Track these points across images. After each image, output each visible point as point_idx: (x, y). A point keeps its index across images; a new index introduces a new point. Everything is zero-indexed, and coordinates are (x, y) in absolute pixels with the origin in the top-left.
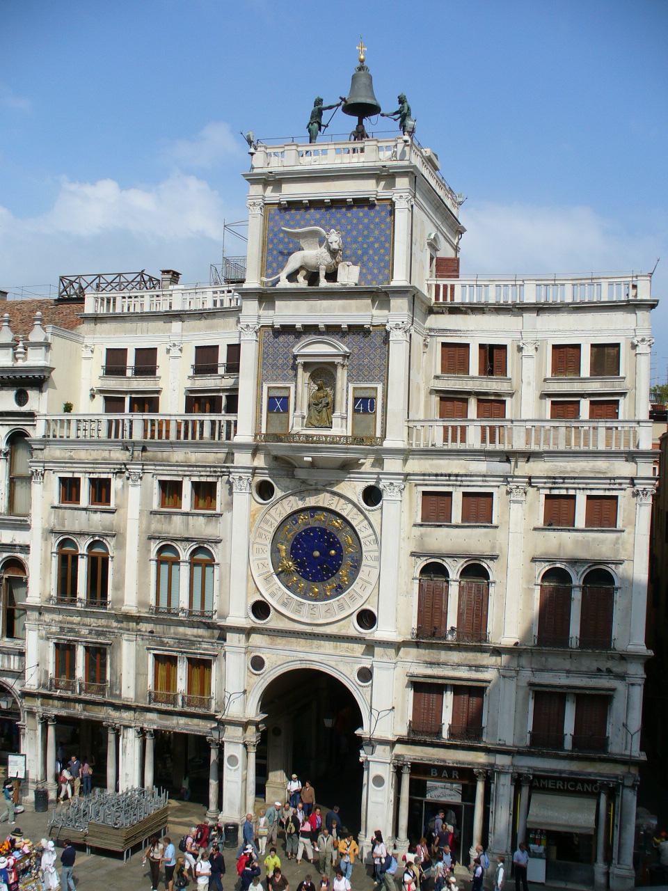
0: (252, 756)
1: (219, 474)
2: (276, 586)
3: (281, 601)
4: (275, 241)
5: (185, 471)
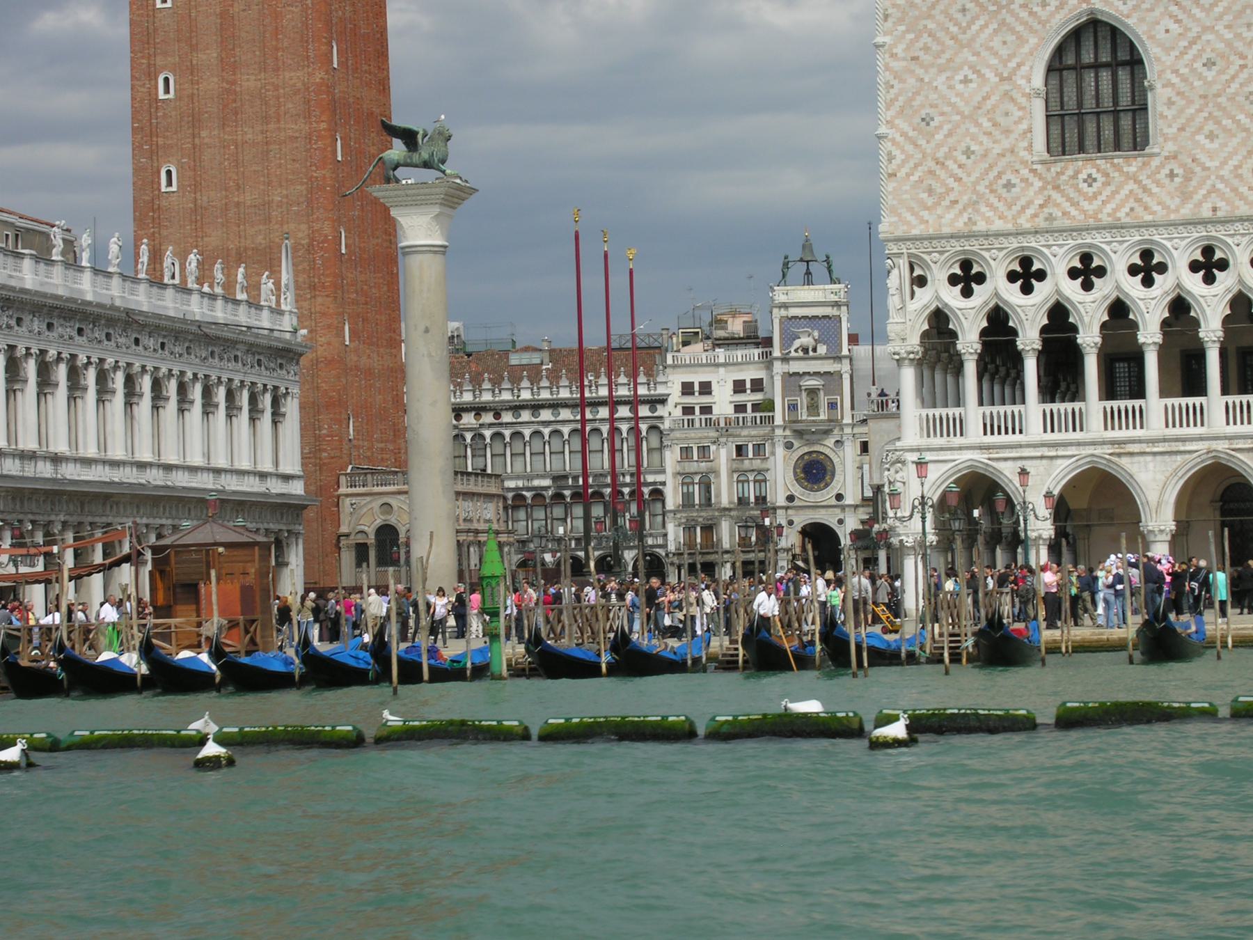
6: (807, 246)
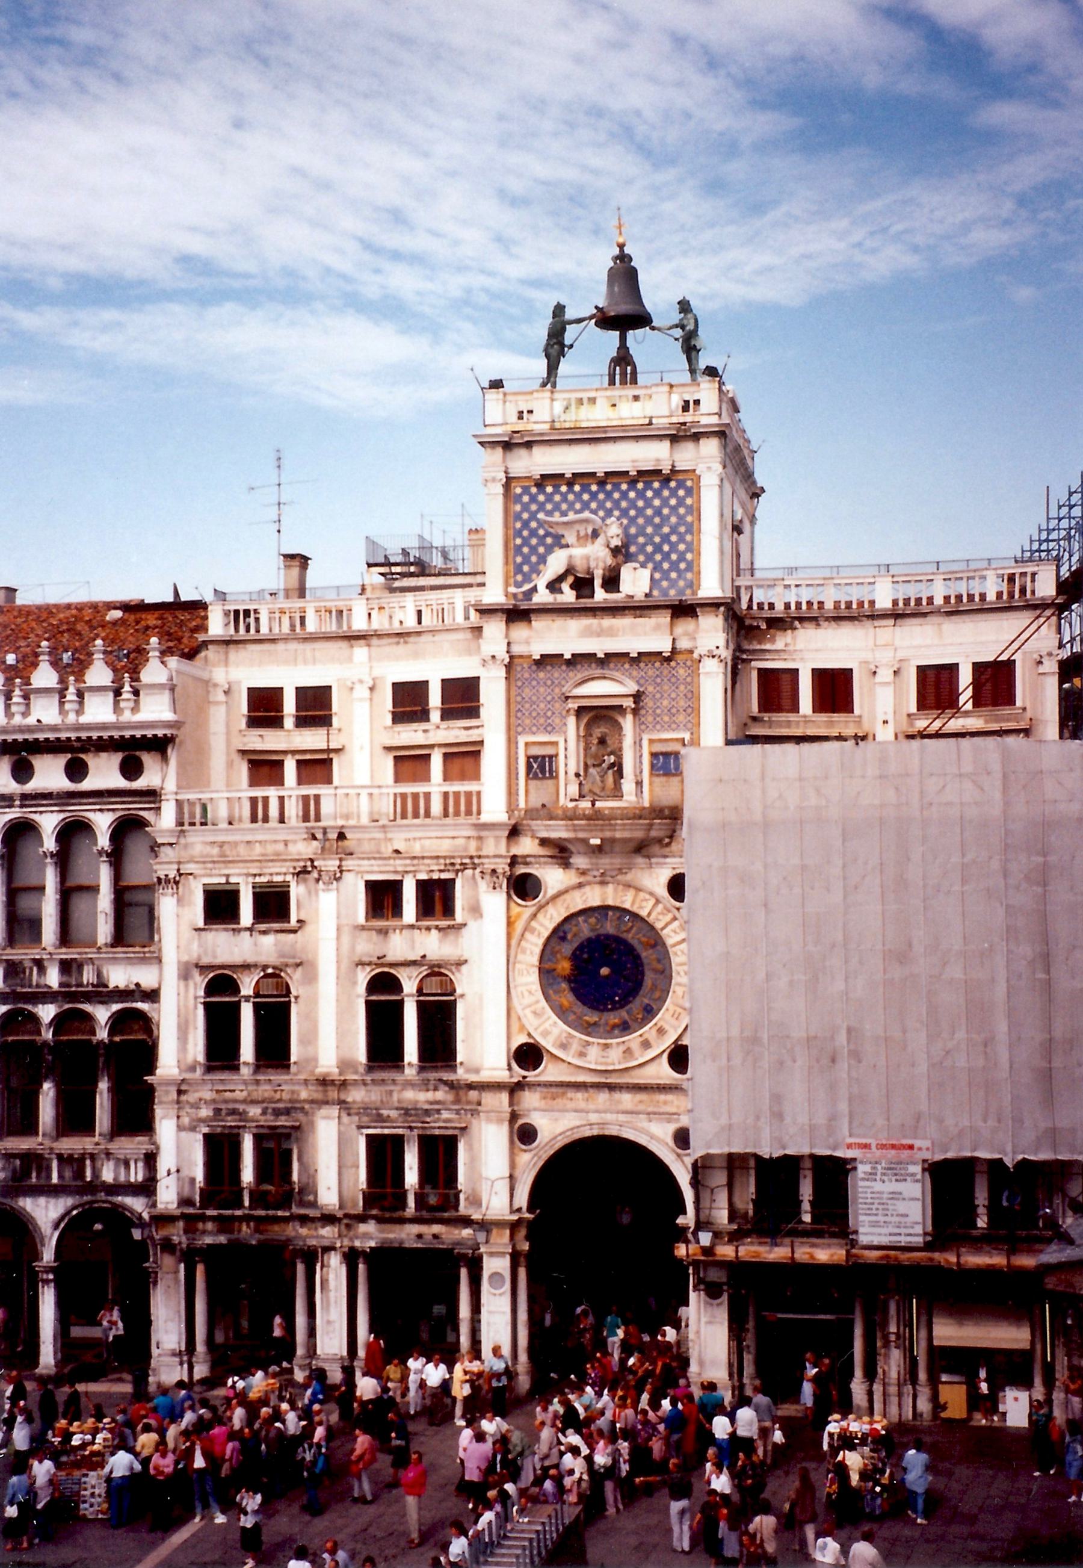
0: (522, 1273)
1: (458, 867)
2: (550, 1022)
3: (558, 1043)
4: (525, 533)
5: (406, 865)
6: (624, 273)
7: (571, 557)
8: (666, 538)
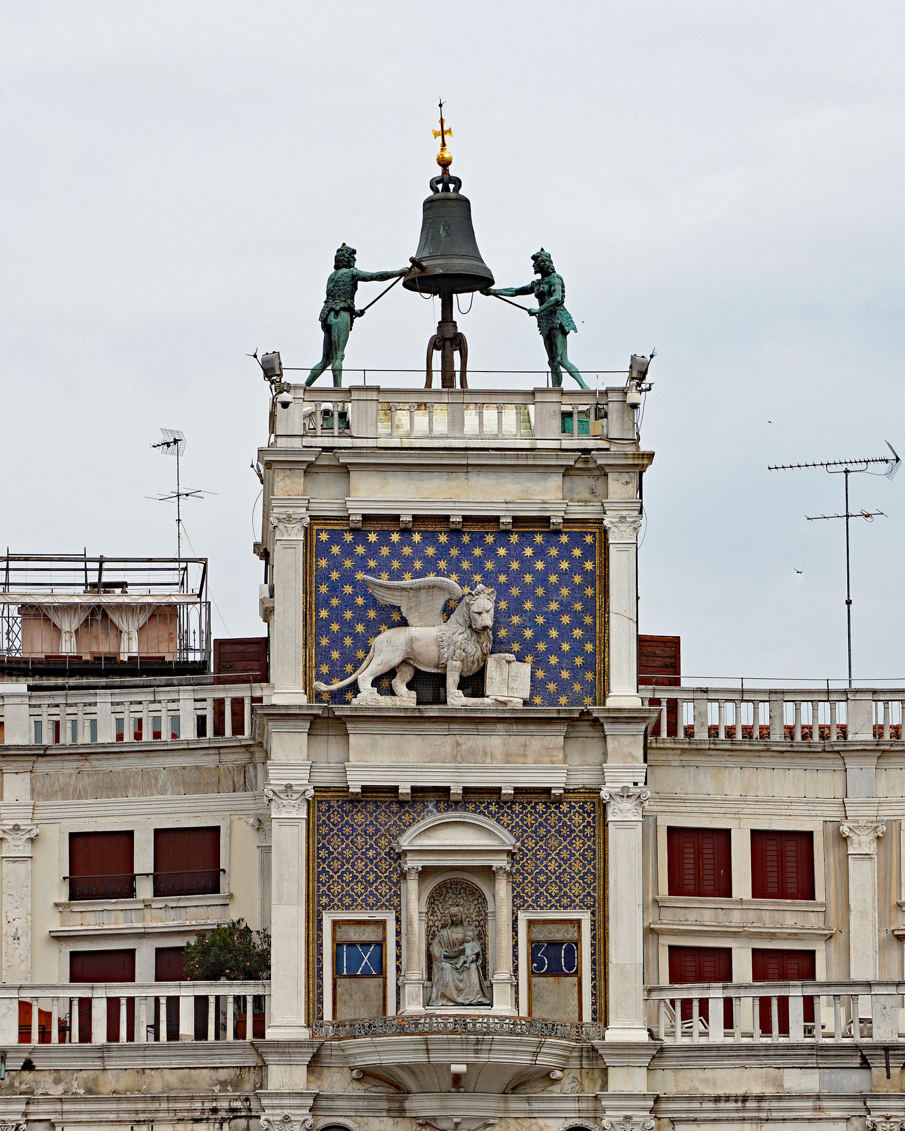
1: (222, 1114)
4: (335, 602)
5: (137, 1112)
7: (411, 641)
8: (553, 619)
